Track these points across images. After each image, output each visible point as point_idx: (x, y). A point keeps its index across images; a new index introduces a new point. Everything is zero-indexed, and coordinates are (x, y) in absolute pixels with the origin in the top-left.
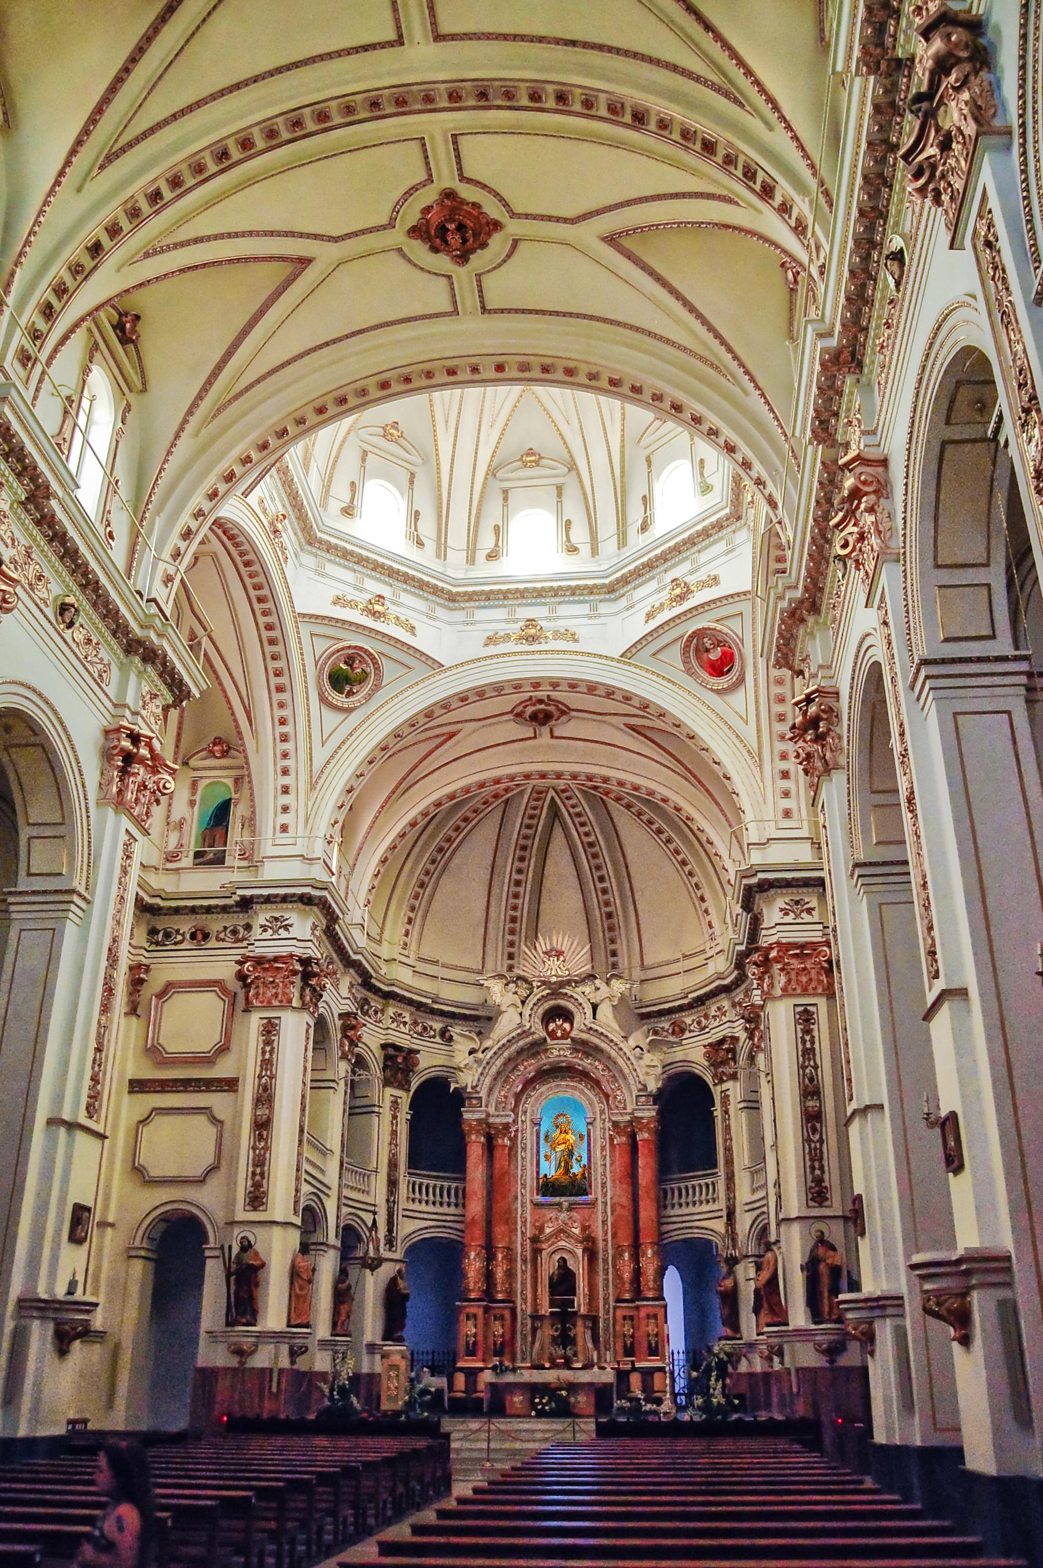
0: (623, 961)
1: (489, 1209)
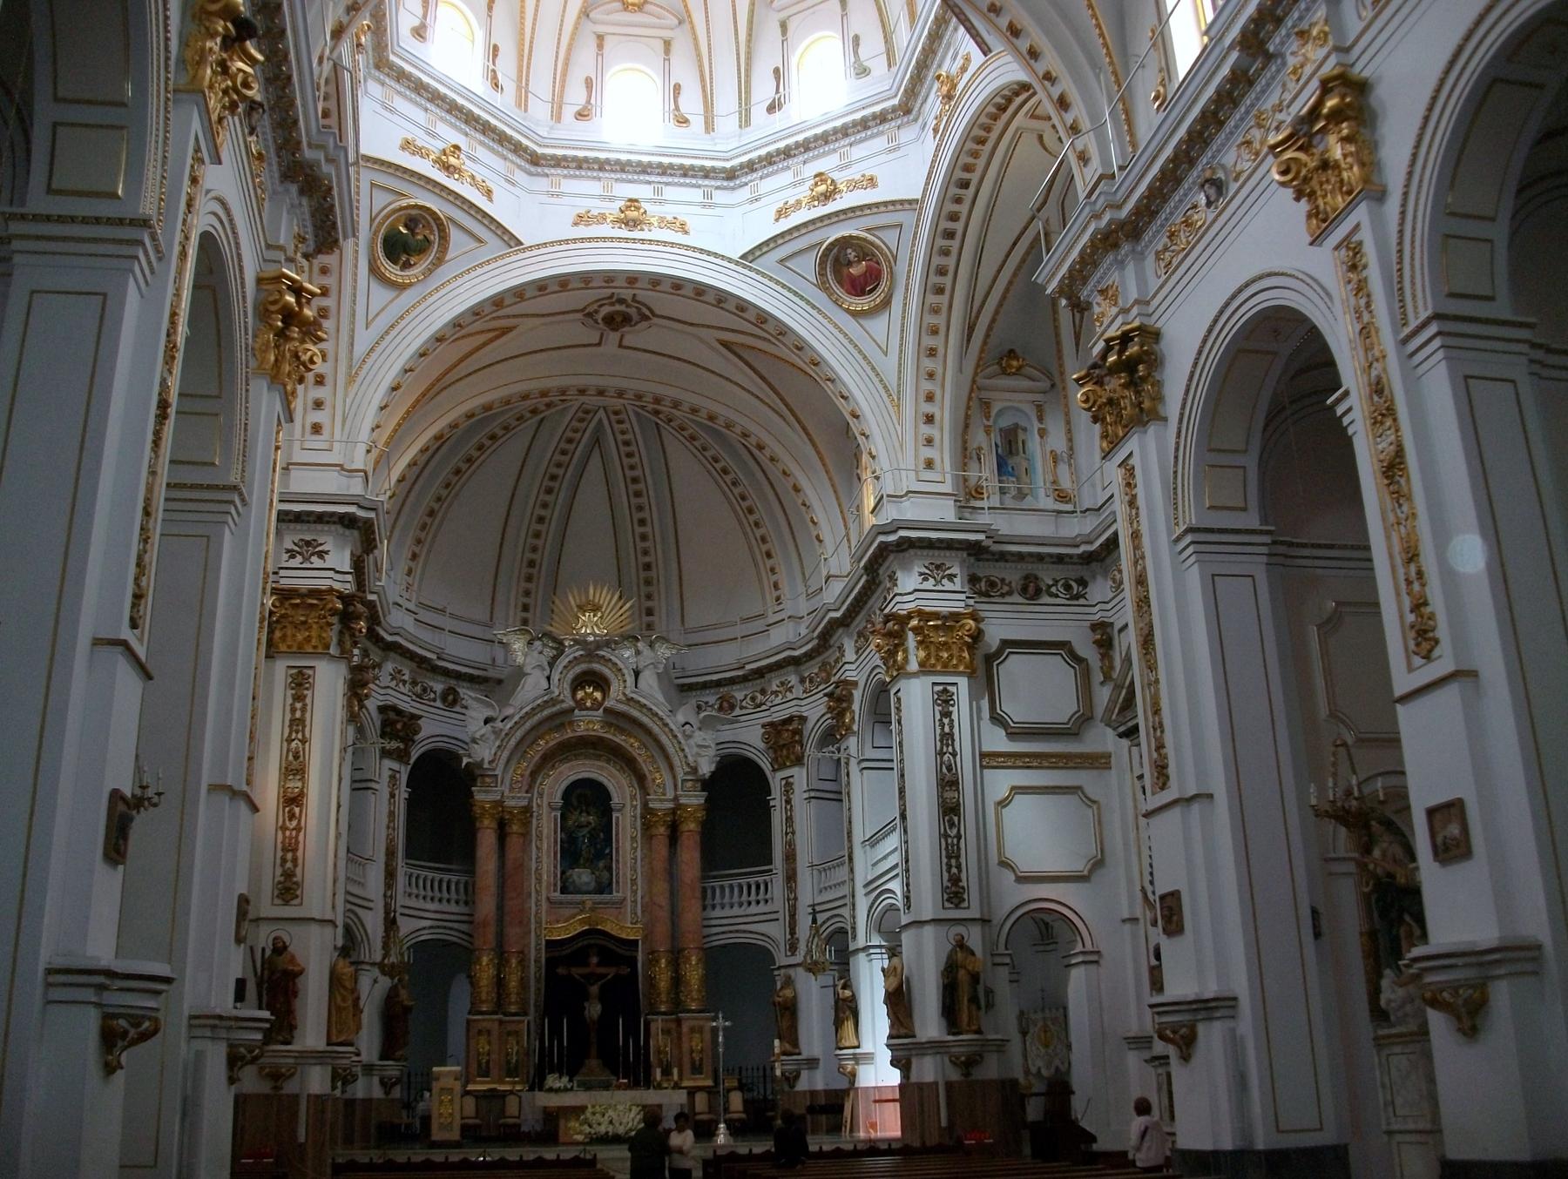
0: (660, 621)
1: (500, 908)
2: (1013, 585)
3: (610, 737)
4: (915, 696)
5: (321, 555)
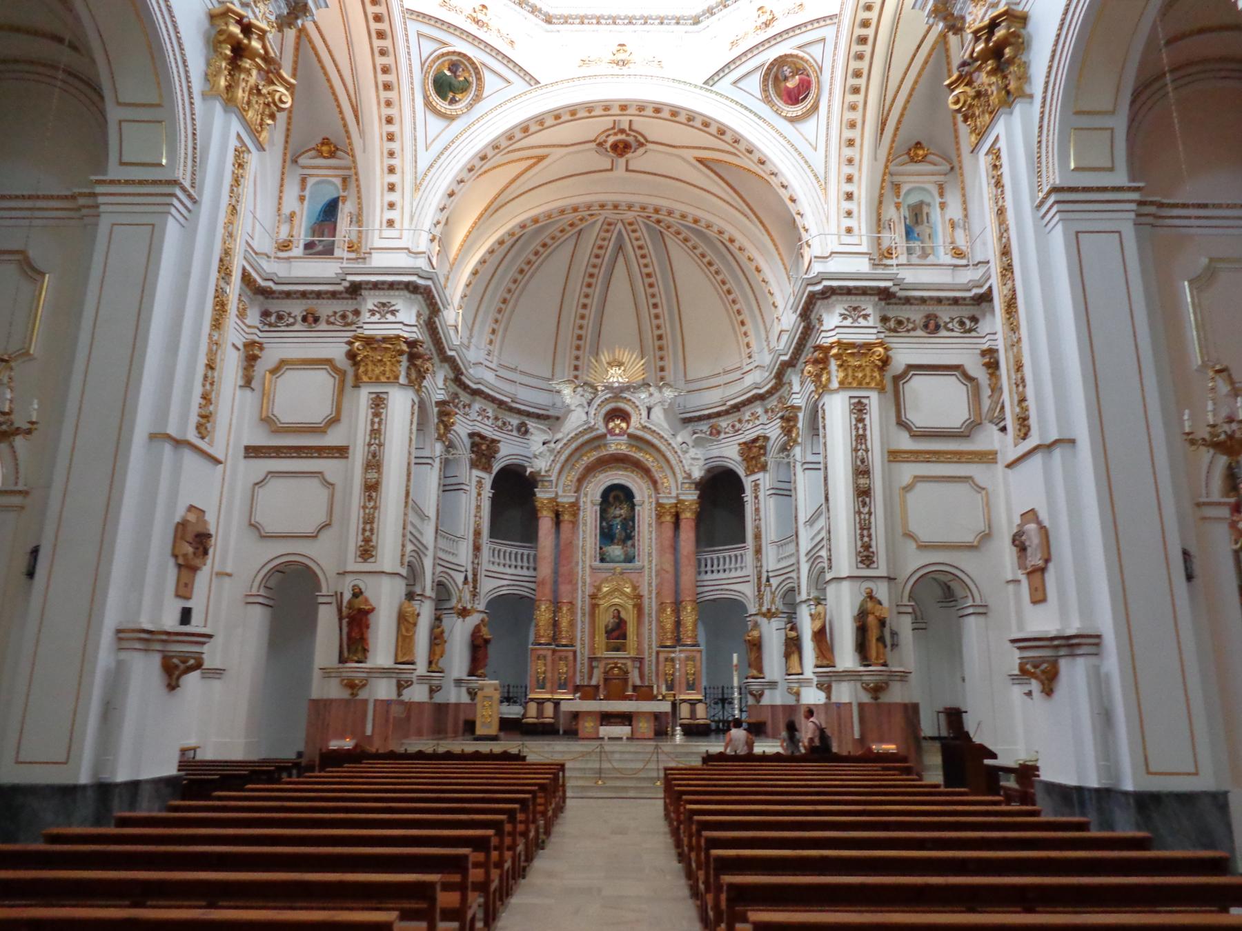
0: (669, 375)
1: (556, 572)
2: (917, 322)
3: (632, 454)
4: (837, 408)
5: (393, 313)
